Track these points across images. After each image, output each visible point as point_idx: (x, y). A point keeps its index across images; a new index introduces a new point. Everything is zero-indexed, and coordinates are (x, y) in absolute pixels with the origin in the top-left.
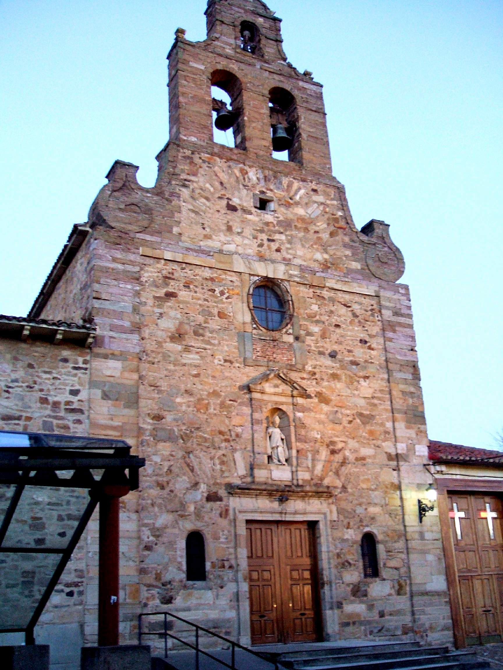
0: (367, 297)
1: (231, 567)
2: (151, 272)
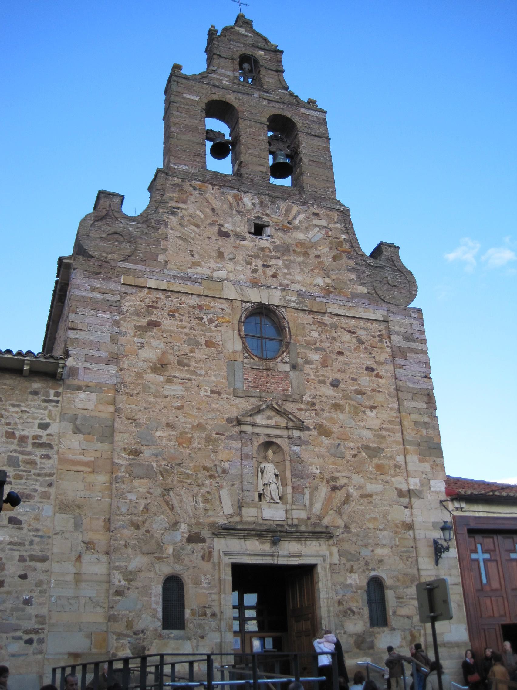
0: (374, 323)
1: (213, 615)
2: (133, 301)
